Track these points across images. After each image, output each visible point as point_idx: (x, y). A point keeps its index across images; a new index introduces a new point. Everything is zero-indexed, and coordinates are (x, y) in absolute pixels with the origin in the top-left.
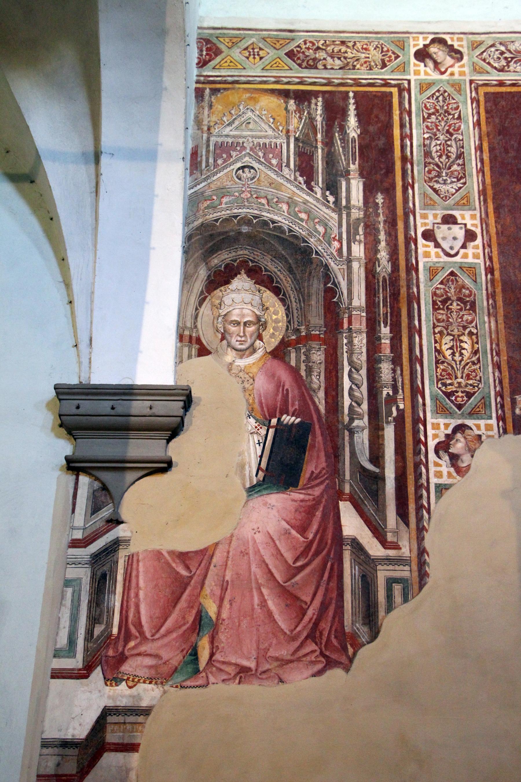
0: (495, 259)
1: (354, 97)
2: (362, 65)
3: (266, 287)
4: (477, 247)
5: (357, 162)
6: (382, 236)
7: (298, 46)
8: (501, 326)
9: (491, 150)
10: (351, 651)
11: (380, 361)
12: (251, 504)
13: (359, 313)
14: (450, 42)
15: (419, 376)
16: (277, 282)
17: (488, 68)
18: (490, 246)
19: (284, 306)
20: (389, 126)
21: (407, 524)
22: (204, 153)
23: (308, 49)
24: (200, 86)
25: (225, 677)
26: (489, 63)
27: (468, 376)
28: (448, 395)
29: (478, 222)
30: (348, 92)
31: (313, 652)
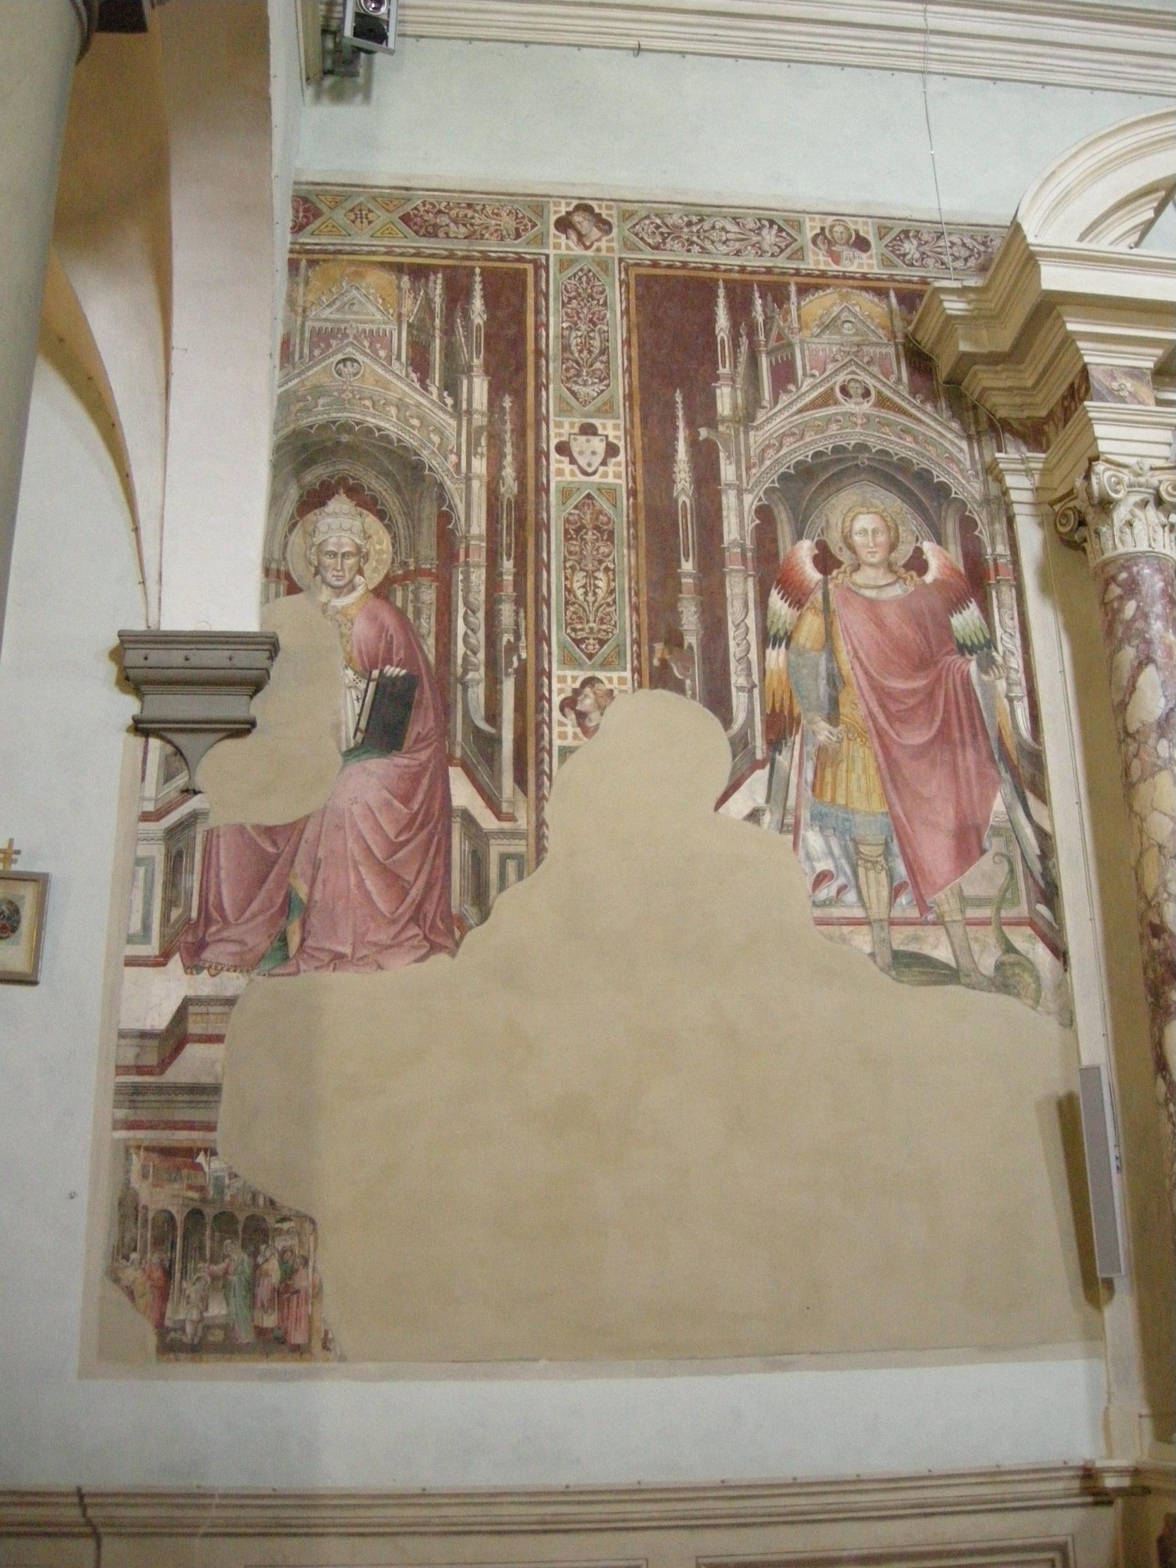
0: (639, 480)
1: (481, 274)
2: (492, 234)
3: (370, 510)
4: (618, 464)
5: (482, 356)
6: (509, 449)
7: (416, 209)
8: (643, 561)
9: (641, 345)
10: (457, 934)
11: (500, 601)
12: (347, 770)
13: (477, 542)
14: (597, 210)
15: (545, 620)
16: (382, 504)
17: (641, 244)
18: (634, 463)
19: (390, 532)
21: (525, 792)
22: (298, 341)
23: (428, 212)
24: (295, 256)
26: (642, 239)
28: (578, 642)
29: (621, 433)
30: (473, 268)
31: (416, 936)
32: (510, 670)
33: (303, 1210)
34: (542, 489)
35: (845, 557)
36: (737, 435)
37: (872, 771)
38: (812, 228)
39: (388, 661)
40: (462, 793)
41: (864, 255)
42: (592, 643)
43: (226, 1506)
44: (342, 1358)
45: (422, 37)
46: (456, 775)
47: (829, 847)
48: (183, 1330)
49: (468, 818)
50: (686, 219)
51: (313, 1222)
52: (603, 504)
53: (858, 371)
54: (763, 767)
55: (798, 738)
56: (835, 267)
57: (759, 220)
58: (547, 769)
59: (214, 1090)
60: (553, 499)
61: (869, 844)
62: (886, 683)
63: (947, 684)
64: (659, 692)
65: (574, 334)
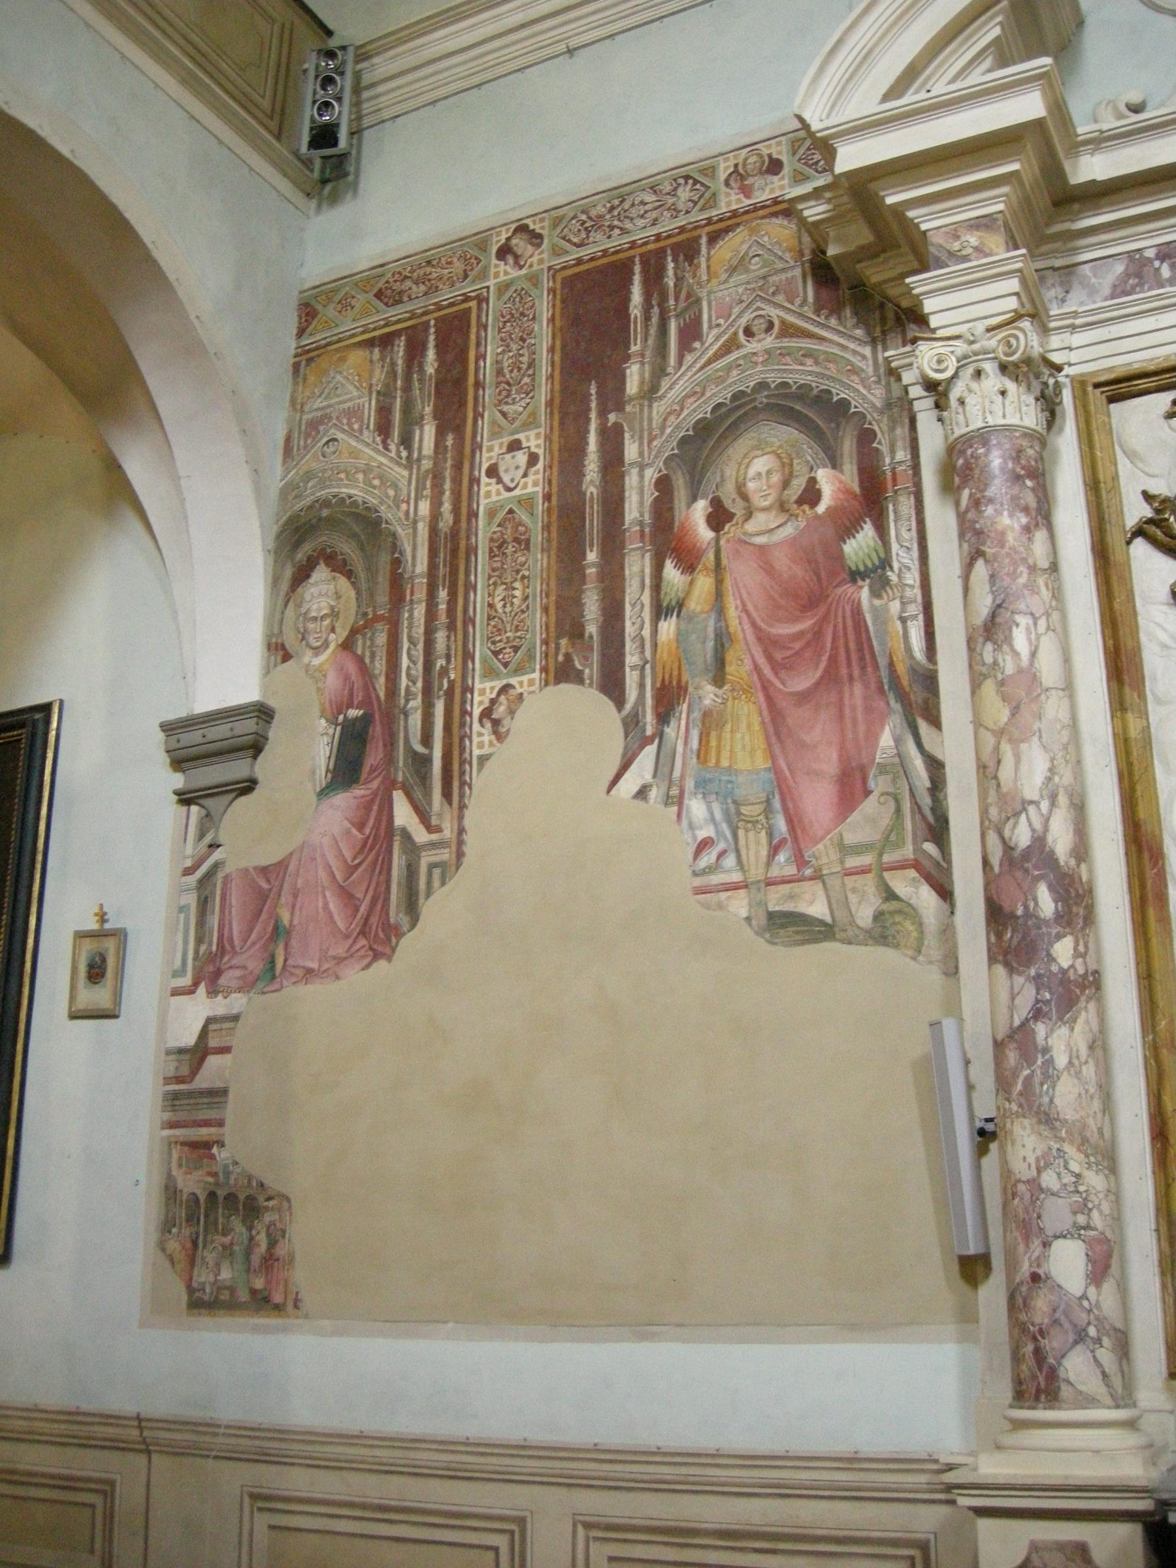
0: (554, 482)
3: (341, 573)
4: (537, 473)
6: (448, 485)
7: (387, 282)
8: (553, 561)
9: (563, 347)
10: (394, 940)
11: (436, 630)
14: (532, 227)
15: (471, 639)
17: (568, 246)
18: (551, 467)
20: (464, 351)
21: (450, 803)
25: (295, 980)
26: (569, 241)
27: (517, 627)
28: (496, 653)
29: (541, 441)
31: (363, 947)
32: (441, 693)
33: (283, 1190)
35: (737, 508)
36: (641, 410)
37: (757, 727)
38: (726, 168)
39: (350, 705)
40: (403, 814)
41: (775, 178)
42: (508, 654)
43: (230, 1435)
44: (307, 1316)
45: (397, 117)
46: (399, 798)
47: (712, 813)
48: (204, 1290)
49: (406, 835)
50: (608, 205)
51: (288, 1200)
52: (523, 516)
53: (763, 306)
54: (652, 742)
55: (685, 706)
56: (749, 202)
57: (675, 180)
58: (468, 779)
59: (224, 1092)
60: (481, 523)
61: (753, 804)
62: (773, 631)
63: (836, 616)
64: (563, 686)
65: (506, 357)
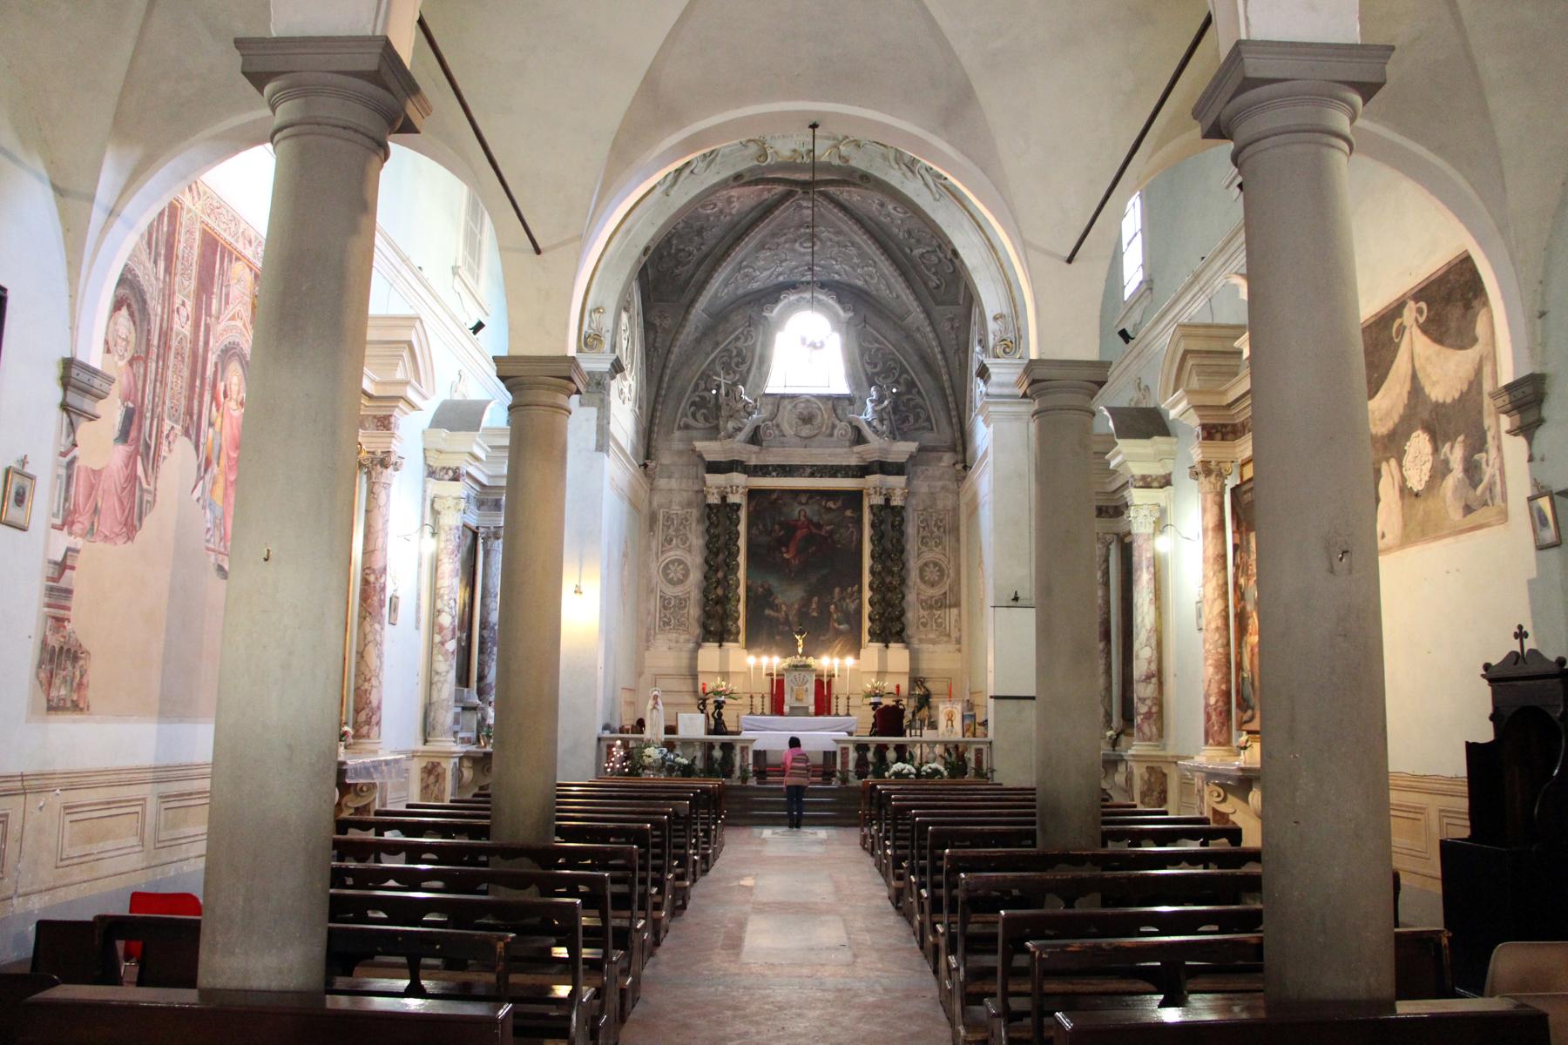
34: (172, 329)
